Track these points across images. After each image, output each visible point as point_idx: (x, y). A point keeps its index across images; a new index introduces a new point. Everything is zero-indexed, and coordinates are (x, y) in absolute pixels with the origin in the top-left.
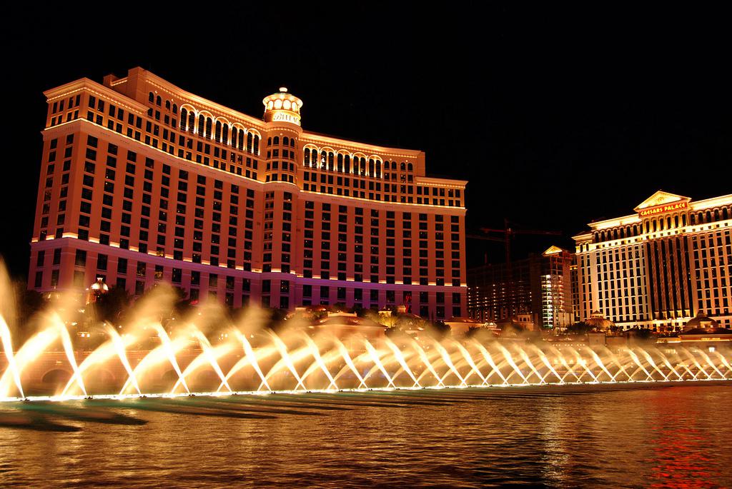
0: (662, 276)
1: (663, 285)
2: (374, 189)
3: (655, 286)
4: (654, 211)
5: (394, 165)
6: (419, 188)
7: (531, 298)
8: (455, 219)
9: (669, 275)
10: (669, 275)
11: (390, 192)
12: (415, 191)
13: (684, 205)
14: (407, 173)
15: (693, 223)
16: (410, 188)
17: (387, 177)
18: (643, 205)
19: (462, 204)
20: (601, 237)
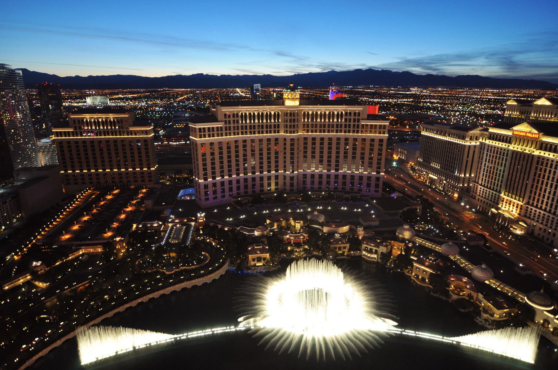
0: (514, 173)
1: (513, 179)
2: (338, 128)
3: (510, 177)
4: (521, 134)
5: (350, 113)
6: (363, 125)
7: (373, 214)
8: (381, 140)
9: (518, 175)
10: (518, 175)
11: (347, 128)
12: (360, 127)
13: (537, 136)
14: (357, 118)
15: (541, 149)
16: (358, 126)
17: (346, 120)
18: (515, 128)
19: (386, 132)
20: (493, 137)
